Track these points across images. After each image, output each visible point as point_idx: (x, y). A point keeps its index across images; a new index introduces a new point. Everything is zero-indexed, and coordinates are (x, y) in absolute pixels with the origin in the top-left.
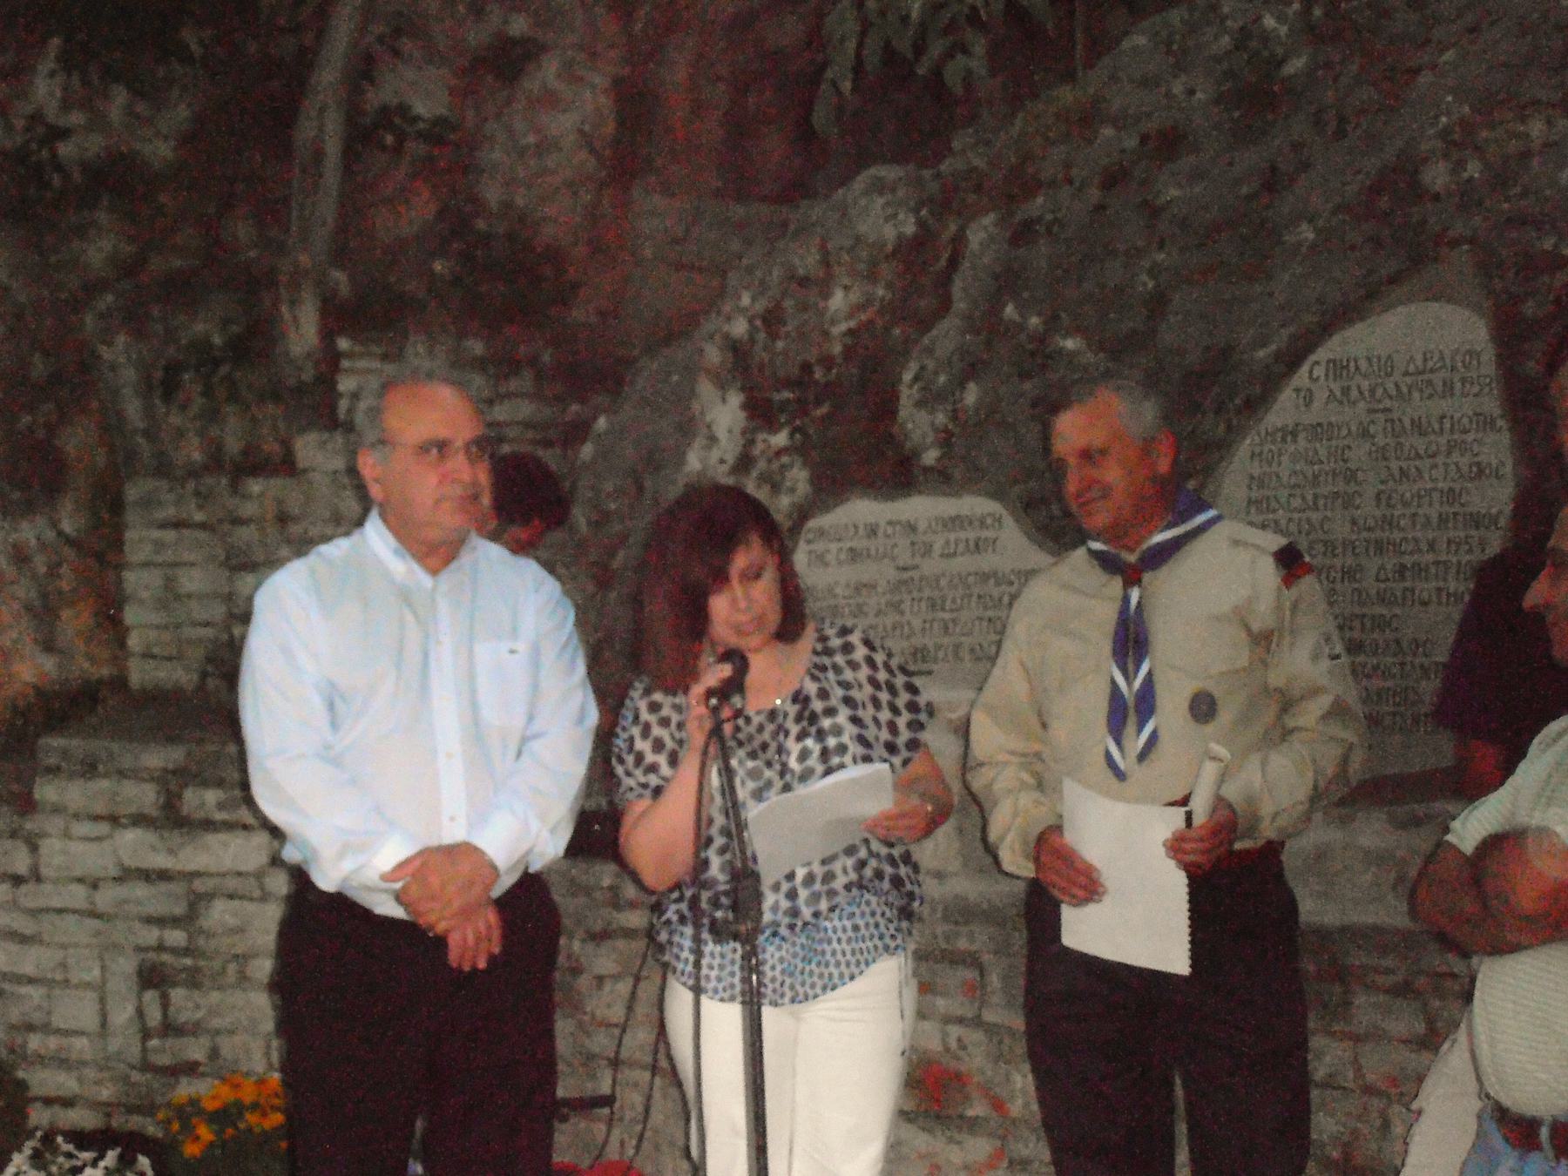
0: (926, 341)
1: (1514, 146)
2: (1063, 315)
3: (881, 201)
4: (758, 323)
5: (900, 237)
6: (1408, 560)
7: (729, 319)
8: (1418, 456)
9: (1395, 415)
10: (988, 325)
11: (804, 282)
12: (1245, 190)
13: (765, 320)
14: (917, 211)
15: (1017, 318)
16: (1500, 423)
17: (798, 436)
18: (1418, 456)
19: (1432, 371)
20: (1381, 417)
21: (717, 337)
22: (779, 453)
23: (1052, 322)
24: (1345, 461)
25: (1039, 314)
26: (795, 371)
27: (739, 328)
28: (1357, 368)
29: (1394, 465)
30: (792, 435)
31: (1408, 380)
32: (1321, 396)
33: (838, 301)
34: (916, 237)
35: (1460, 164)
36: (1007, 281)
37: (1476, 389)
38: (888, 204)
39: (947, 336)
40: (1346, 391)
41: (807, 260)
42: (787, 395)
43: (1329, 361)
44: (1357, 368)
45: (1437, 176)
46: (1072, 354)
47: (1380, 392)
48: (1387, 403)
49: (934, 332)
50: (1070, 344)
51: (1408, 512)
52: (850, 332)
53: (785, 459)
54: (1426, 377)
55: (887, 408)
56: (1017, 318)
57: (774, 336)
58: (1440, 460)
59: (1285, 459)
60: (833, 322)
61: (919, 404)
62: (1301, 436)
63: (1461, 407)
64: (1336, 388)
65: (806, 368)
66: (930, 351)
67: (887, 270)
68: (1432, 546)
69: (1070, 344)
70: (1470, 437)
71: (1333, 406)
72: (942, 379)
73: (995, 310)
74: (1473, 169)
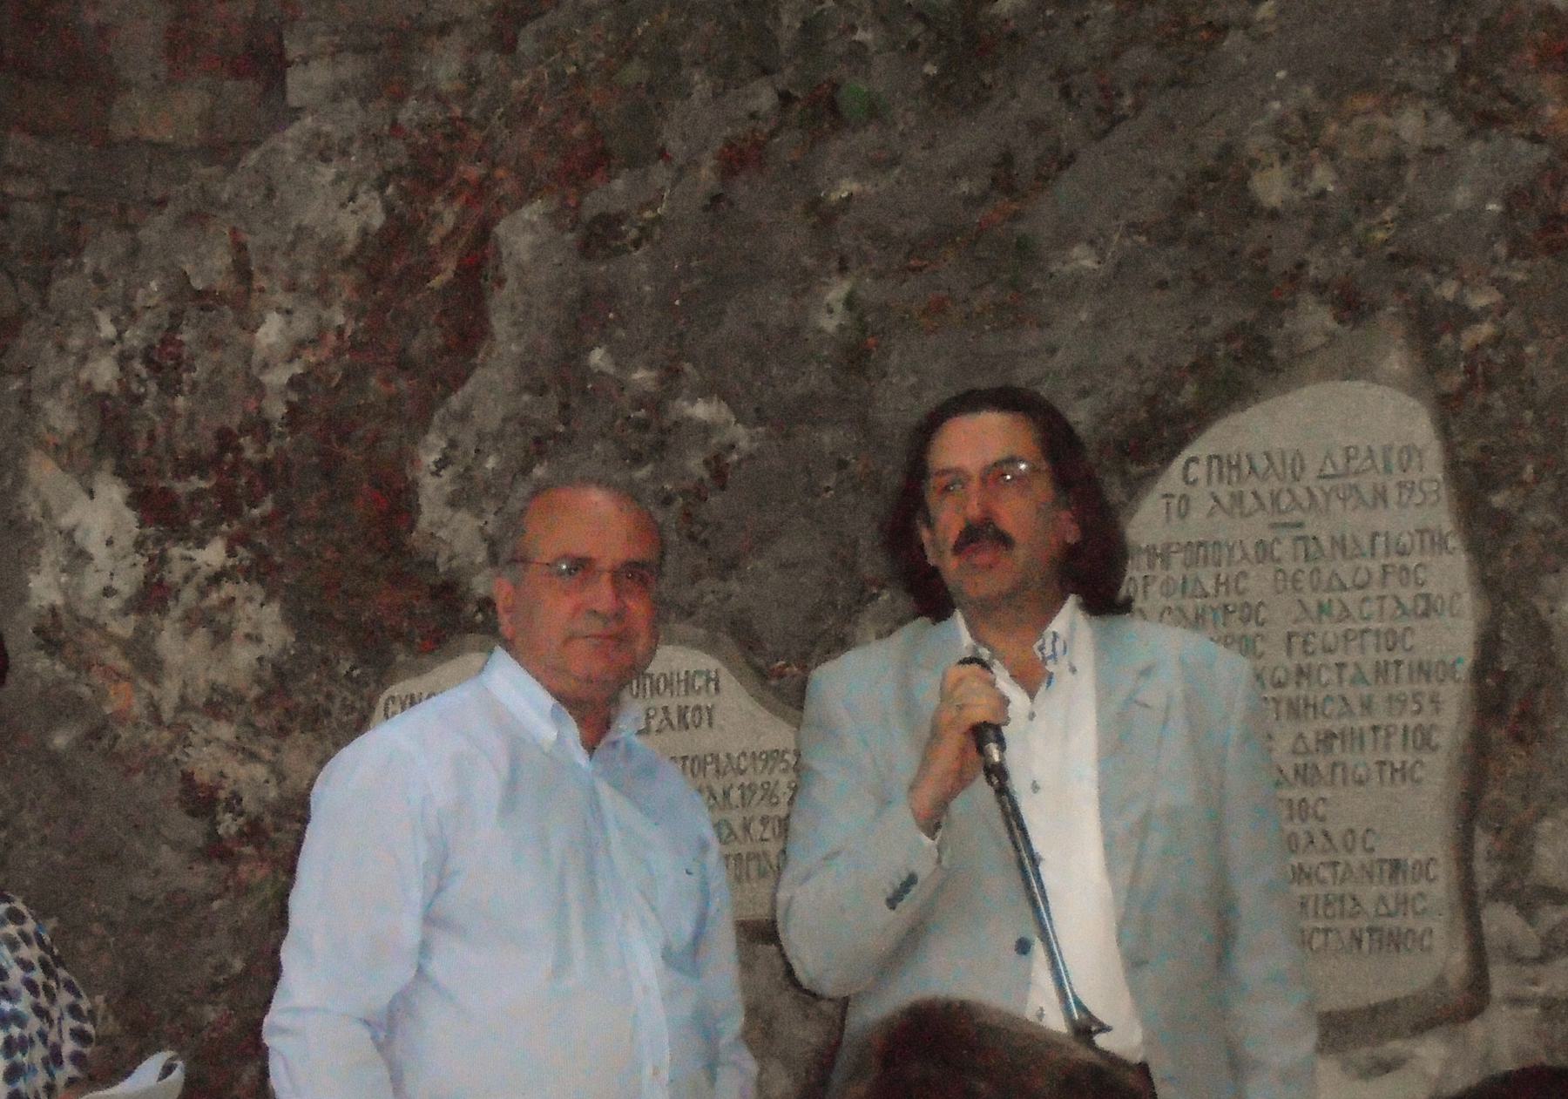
0: (455, 401)
1: (1380, 147)
2: (688, 367)
3: (328, 173)
4: (138, 365)
5: (364, 231)
6: (1335, 726)
7: (83, 359)
8: (1344, 588)
9: (1308, 532)
10: (560, 377)
11: (206, 299)
12: (964, 187)
13: (148, 361)
14: (381, 187)
15: (611, 370)
16: (1453, 542)
17: (242, 551)
18: (1344, 588)
19: (1357, 473)
20: (1287, 537)
21: (65, 390)
22: (216, 579)
23: (671, 374)
24: (1240, 593)
25: (650, 365)
26: (209, 446)
27: (104, 373)
28: (1253, 469)
29: (1311, 602)
30: (231, 553)
31: (1327, 485)
32: (1201, 503)
33: (271, 332)
34: (383, 230)
35: (1305, 171)
36: (587, 313)
37: (1418, 498)
38: (340, 177)
39: (492, 390)
40: (1238, 498)
41: (210, 266)
42: (196, 483)
43: (1210, 458)
44: (1253, 469)
45: (1272, 187)
46: (707, 429)
47: (1285, 500)
48: (1297, 515)
49: (469, 388)
50: (701, 411)
51: (1333, 659)
52: (294, 383)
53: (228, 589)
54: (1353, 481)
56: (611, 370)
57: (170, 387)
58: (1373, 591)
59: (1154, 588)
60: (265, 366)
61: (453, 503)
62: (1177, 559)
63: (1399, 521)
64: (1223, 491)
65: (226, 439)
66: (463, 417)
67: (345, 284)
68: (1367, 706)
69: (701, 411)
70: (1412, 562)
71: (1220, 516)
72: (491, 463)
73: (573, 357)
74: (1323, 177)
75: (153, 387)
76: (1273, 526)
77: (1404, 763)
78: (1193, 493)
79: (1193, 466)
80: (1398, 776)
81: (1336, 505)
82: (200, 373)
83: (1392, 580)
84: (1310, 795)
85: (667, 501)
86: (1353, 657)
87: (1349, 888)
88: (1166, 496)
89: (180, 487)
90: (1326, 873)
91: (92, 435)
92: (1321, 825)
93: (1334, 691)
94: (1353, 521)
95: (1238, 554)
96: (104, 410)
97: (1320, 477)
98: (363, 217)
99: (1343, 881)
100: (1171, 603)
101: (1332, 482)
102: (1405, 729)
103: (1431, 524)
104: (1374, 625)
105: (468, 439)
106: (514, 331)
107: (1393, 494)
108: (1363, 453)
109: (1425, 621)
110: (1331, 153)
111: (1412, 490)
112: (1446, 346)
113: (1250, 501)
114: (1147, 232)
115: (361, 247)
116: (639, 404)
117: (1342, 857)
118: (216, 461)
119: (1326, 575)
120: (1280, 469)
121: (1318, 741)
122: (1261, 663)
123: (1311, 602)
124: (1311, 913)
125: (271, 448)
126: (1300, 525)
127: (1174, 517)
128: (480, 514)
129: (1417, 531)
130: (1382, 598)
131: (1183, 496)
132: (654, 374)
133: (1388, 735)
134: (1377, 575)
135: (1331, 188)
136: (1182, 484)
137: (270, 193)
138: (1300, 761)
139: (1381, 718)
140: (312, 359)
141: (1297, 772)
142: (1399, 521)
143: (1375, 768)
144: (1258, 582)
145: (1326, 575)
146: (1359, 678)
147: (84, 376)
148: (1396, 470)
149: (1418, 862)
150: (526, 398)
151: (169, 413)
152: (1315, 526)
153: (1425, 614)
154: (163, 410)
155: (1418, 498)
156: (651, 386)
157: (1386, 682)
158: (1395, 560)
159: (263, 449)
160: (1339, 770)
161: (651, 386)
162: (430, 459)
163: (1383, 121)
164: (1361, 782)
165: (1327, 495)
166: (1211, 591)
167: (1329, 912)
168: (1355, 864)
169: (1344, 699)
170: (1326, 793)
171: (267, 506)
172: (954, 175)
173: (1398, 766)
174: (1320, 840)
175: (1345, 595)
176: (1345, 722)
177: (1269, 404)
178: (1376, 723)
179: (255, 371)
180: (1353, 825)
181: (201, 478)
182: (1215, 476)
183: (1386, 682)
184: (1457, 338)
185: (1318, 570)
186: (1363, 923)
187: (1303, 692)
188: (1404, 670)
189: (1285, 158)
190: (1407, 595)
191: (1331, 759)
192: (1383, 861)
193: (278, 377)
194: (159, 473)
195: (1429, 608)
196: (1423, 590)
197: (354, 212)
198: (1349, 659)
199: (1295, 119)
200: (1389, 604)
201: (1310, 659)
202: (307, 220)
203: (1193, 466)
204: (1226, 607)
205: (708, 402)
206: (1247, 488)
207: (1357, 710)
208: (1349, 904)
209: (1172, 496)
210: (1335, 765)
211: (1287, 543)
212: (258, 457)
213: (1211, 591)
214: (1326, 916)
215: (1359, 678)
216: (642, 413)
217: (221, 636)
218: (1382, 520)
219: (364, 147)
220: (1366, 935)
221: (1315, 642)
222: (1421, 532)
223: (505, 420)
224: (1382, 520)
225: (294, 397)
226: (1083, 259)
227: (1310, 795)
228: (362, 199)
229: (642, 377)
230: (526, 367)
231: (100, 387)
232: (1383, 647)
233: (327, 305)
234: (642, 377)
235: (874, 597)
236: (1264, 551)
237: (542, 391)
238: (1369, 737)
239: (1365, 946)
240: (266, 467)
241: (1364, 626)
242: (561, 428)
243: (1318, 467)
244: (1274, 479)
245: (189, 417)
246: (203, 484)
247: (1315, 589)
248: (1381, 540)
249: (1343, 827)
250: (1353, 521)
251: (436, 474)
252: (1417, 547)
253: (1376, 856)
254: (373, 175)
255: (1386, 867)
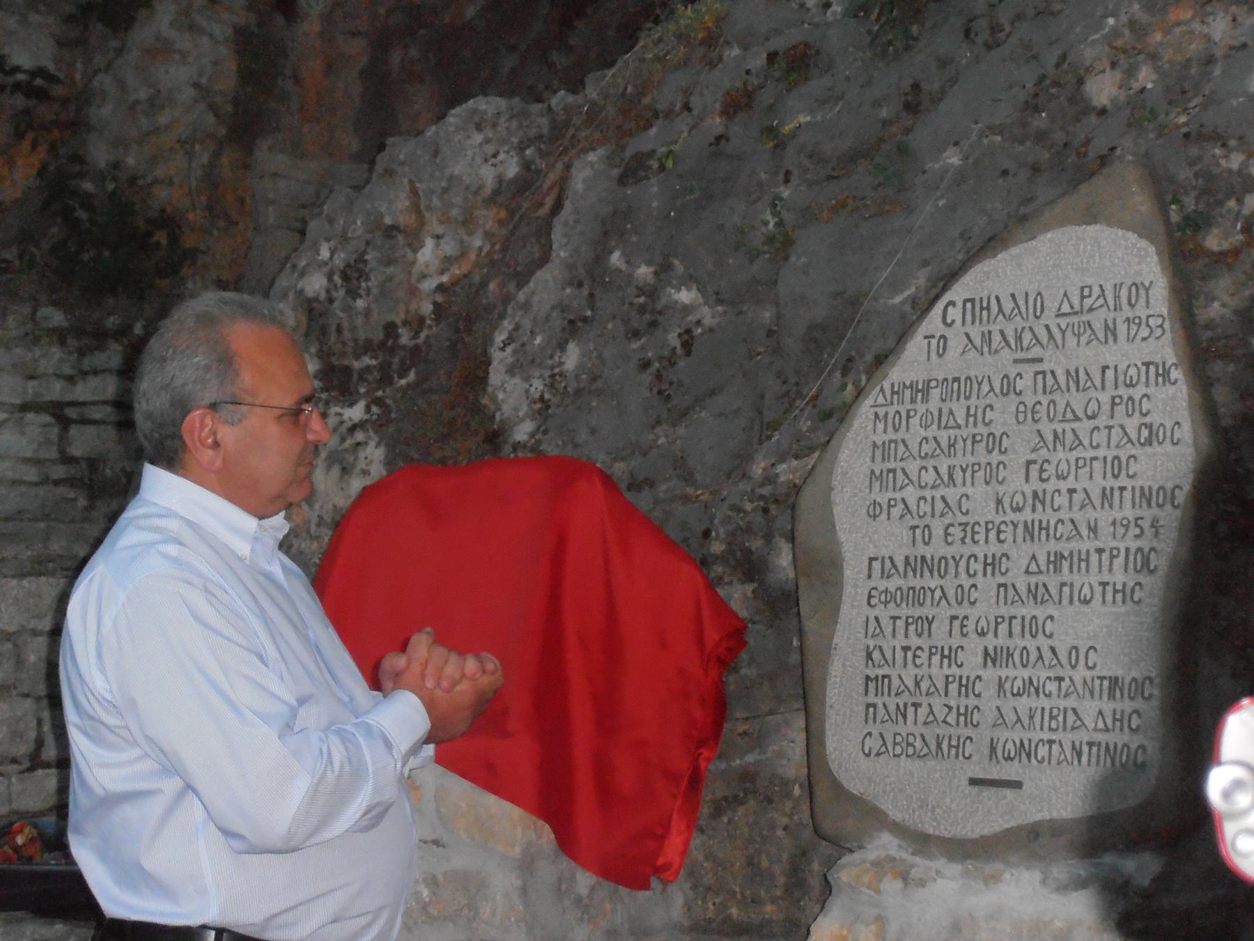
0: (521, 297)
1: (1194, 47)
2: (677, 262)
3: (478, 138)
4: (336, 278)
5: (500, 179)
6: (1065, 547)
7: (303, 274)
8: (1077, 419)
9: (1045, 366)
10: (592, 276)
11: (391, 231)
12: (884, 113)
13: (346, 277)
14: (521, 148)
15: (623, 267)
16: (1175, 374)
17: (375, 409)
18: (1077, 419)
19: (1091, 310)
20: (1028, 371)
21: (291, 295)
22: (353, 429)
23: (664, 269)
24: (986, 425)
25: (649, 263)
26: (379, 335)
27: (315, 284)
28: (1000, 310)
29: (1047, 430)
30: (368, 409)
31: (1063, 322)
32: (956, 343)
33: (427, 254)
34: (515, 180)
35: (1131, 72)
36: (615, 226)
37: (1144, 332)
38: (487, 141)
39: (546, 288)
40: (987, 337)
41: (394, 206)
42: (367, 361)
43: (966, 301)
44: (1000, 310)
45: (1103, 89)
46: (687, 309)
47: (1027, 337)
48: (1036, 352)
49: (532, 285)
50: (685, 296)
51: (1064, 486)
52: (441, 288)
53: (359, 436)
54: (1085, 318)
55: (475, 376)
56: (623, 267)
57: (353, 294)
58: (1102, 421)
59: (915, 421)
60: (424, 276)
61: (511, 371)
62: (935, 394)
63: (1125, 354)
64: (975, 332)
65: (391, 329)
66: (526, 306)
67: (488, 218)
68: (1093, 529)
69: (685, 296)
70: (1137, 393)
71: (972, 354)
72: (538, 340)
73: (600, 259)
74: (1146, 77)
75: (342, 292)
76: (1016, 361)
77: (1124, 585)
78: (949, 333)
79: (950, 308)
80: (1119, 596)
81: (1071, 341)
82: (374, 282)
83: (1120, 410)
84: (1041, 613)
85: (645, 365)
86: (1084, 483)
87: (1071, 702)
88: (926, 337)
89: (357, 365)
90: (1051, 687)
91: (304, 327)
92: (1050, 642)
93: (1065, 516)
94: (1087, 356)
95: (985, 388)
96: (311, 310)
97: (1057, 316)
98: (500, 169)
99: (1066, 695)
100: (930, 434)
101: (1068, 320)
102: (1127, 550)
103: (1158, 359)
104: (1101, 453)
105: (527, 324)
106: (564, 241)
107: (1122, 328)
108: (1096, 290)
109: (1148, 449)
110: (1153, 57)
111: (1140, 324)
112: (1229, 210)
113: (997, 338)
114: (1001, 133)
115: (496, 192)
116: (641, 291)
117: (1066, 672)
118: (382, 345)
119: (1061, 407)
120: (1023, 309)
121: (1049, 562)
122: (1001, 489)
123: (1047, 430)
124: (1038, 727)
125: (423, 335)
126: (1040, 360)
127: (933, 355)
128: (527, 379)
129: (1143, 364)
130: (1110, 428)
131: (943, 337)
132: (652, 269)
133: (1112, 557)
134: (1106, 407)
135: (1149, 86)
136: (942, 326)
137: (436, 153)
138: (1033, 580)
139: (1106, 541)
140: (457, 272)
141: (1029, 591)
142: (1125, 354)
143: (1098, 589)
144: (1002, 415)
145: (1061, 407)
146: (1087, 503)
147: (300, 286)
148: (1125, 307)
149: (1134, 679)
150: (568, 291)
151: (348, 309)
152: (1055, 362)
153: (1149, 442)
154: (348, 309)
155: (1144, 332)
156: (651, 279)
157: (1111, 506)
158: (1122, 391)
159: (416, 336)
160: (1066, 590)
161: (651, 279)
162: (500, 337)
163: (1196, 26)
164: (1086, 602)
165: (1063, 332)
166: (961, 421)
167: (1054, 725)
168: (1078, 679)
169: (1072, 521)
170: (1051, 610)
171: (412, 376)
172: (877, 104)
173: (1119, 587)
174: (1047, 655)
175: (1075, 425)
176: (1073, 545)
177: (1015, 250)
178: (1101, 545)
179: (413, 280)
180: (1076, 643)
181: (372, 357)
182: (969, 318)
183: (1111, 506)
184: (1240, 201)
185: (1053, 402)
186: (1083, 736)
187: (1037, 516)
188: (1127, 495)
189: (1114, 65)
190: (1132, 425)
191: (1059, 579)
192: (1102, 678)
193: (429, 285)
194: (344, 354)
195: (1151, 437)
196: (1148, 420)
197: (494, 165)
198: (1079, 487)
199: (1127, 32)
200: (1116, 432)
201: (1045, 485)
202: (457, 170)
203: (950, 308)
204: (974, 436)
205: (689, 289)
206: (995, 328)
207: (1085, 533)
208: (1071, 718)
209: (933, 337)
210: (1063, 584)
211: (1028, 377)
212: (412, 343)
213: (961, 421)
214: (1050, 729)
215: (1087, 503)
216: (642, 300)
217: (346, 471)
218: (1113, 354)
219: (509, 120)
220: (1085, 749)
221: (1050, 469)
222: (1147, 364)
223: (553, 308)
224: (1113, 354)
225: (439, 299)
226: (953, 158)
227: (1041, 613)
228: (502, 156)
229: (644, 272)
230: (571, 267)
231: (310, 293)
232: (1109, 475)
233: (470, 234)
234: (644, 272)
235: (769, 438)
236: (1009, 387)
237: (580, 285)
238: (1094, 558)
239: (1084, 759)
240: (415, 350)
241: (1093, 453)
242: (589, 313)
243: (1057, 305)
244: (1018, 318)
245: (363, 314)
246: (374, 362)
247: (1051, 420)
248: (1110, 374)
249: (1070, 641)
250: (1087, 356)
251: (502, 349)
252: (1143, 379)
253: (1096, 673)
254: (515, 140)
255: (1106, 683)
